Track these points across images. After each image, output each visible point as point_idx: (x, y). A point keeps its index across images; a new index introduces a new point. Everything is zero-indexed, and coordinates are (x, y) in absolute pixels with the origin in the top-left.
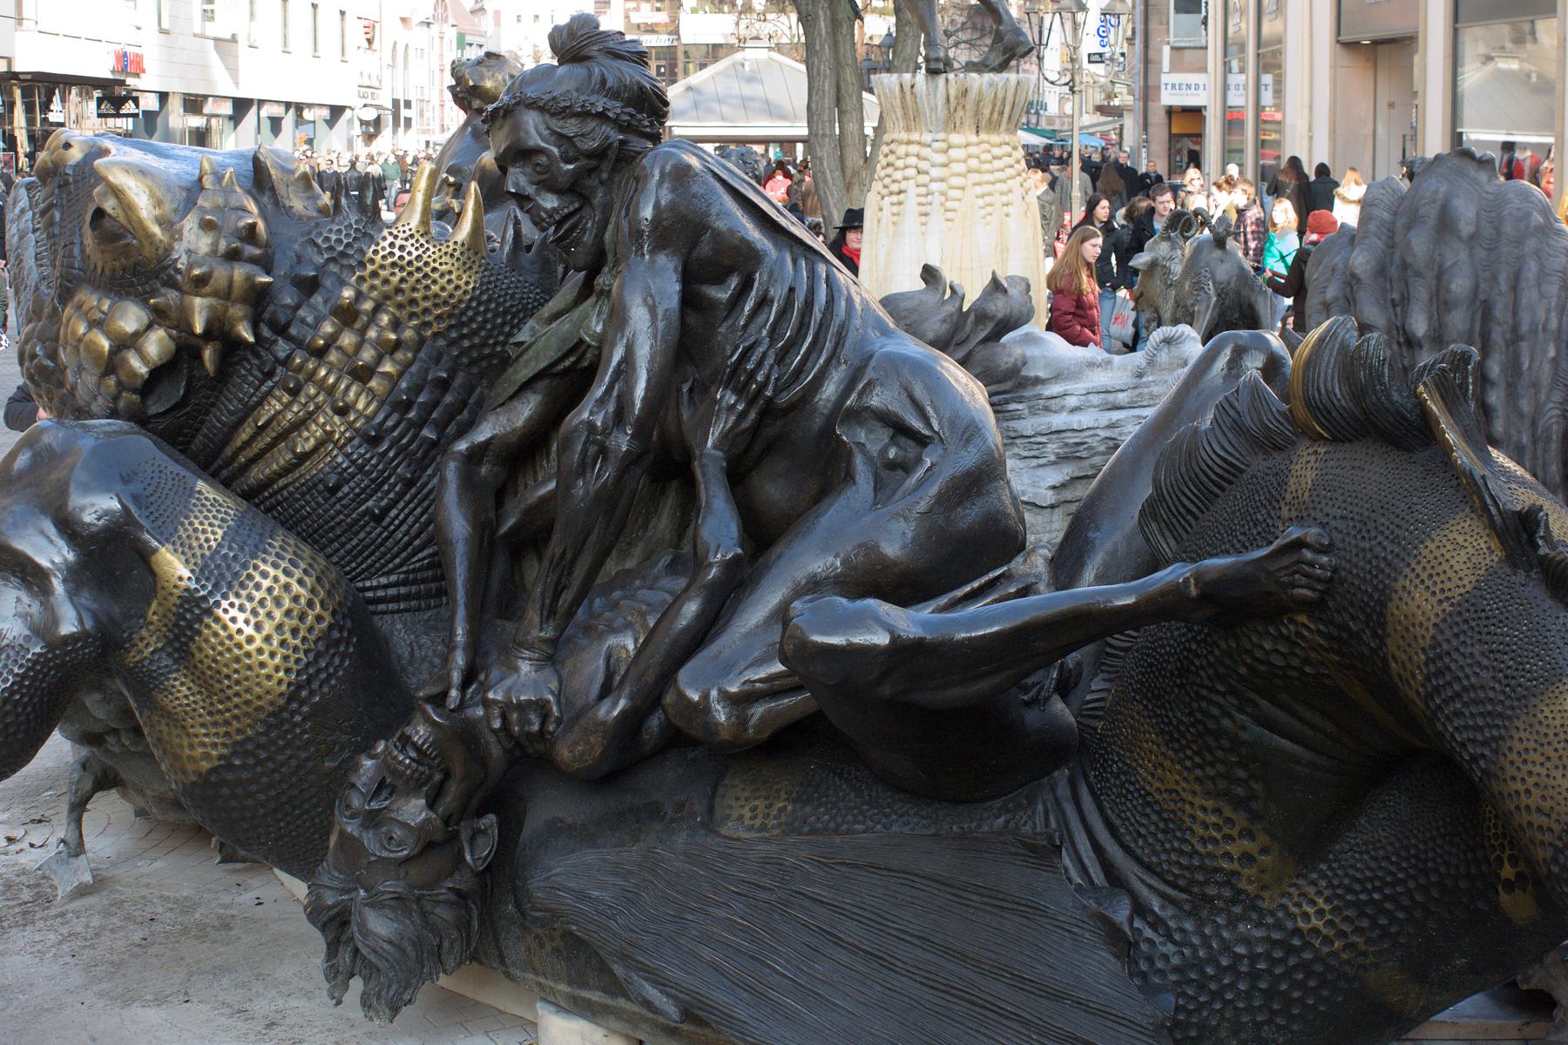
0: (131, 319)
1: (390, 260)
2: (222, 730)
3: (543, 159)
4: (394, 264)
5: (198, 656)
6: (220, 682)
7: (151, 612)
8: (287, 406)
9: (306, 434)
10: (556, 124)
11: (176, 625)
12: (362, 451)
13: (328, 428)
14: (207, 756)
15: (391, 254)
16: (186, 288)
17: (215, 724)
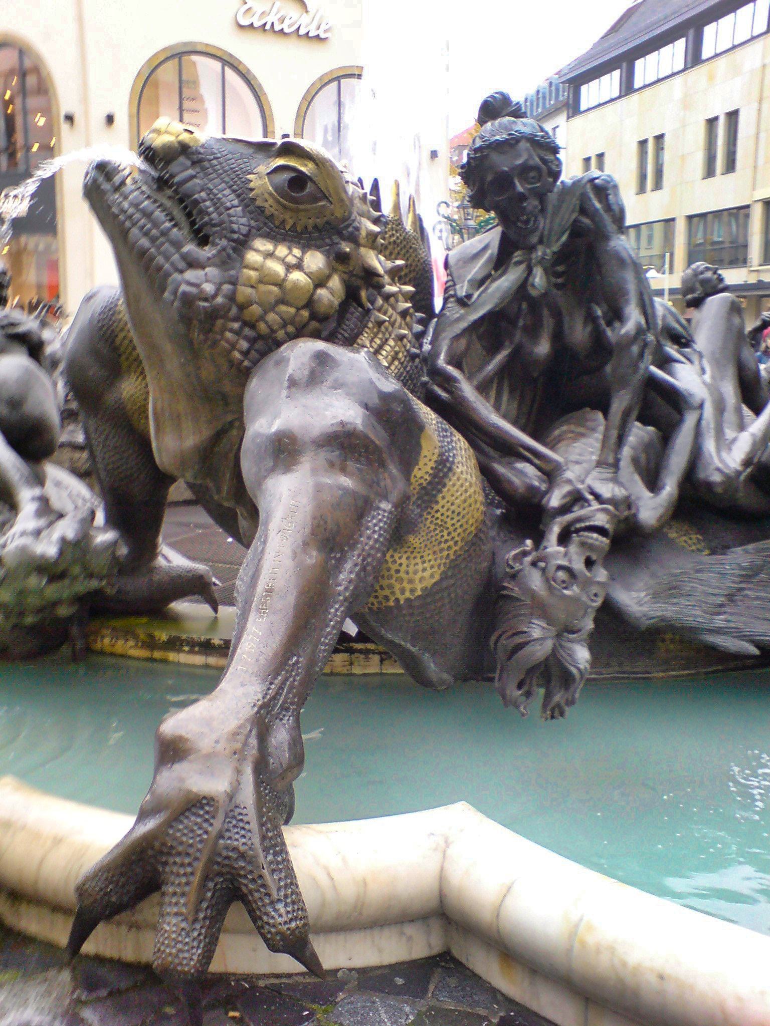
0: (315, 261)
1: (392, 239)
2: (445, 553)
3: (532, 174)
4: (395, 242)
5: (442, 502)
6: (452, 519)
7: (413, 476)
8: (376, 335)
9: (384, 353)
10: (542, 153)
11: (430, 483)
12: (410, 364)
13: (397, 349)
14: (432, 576)
15: (393, 235)
16: (362, 241)
17: (442, 550)
